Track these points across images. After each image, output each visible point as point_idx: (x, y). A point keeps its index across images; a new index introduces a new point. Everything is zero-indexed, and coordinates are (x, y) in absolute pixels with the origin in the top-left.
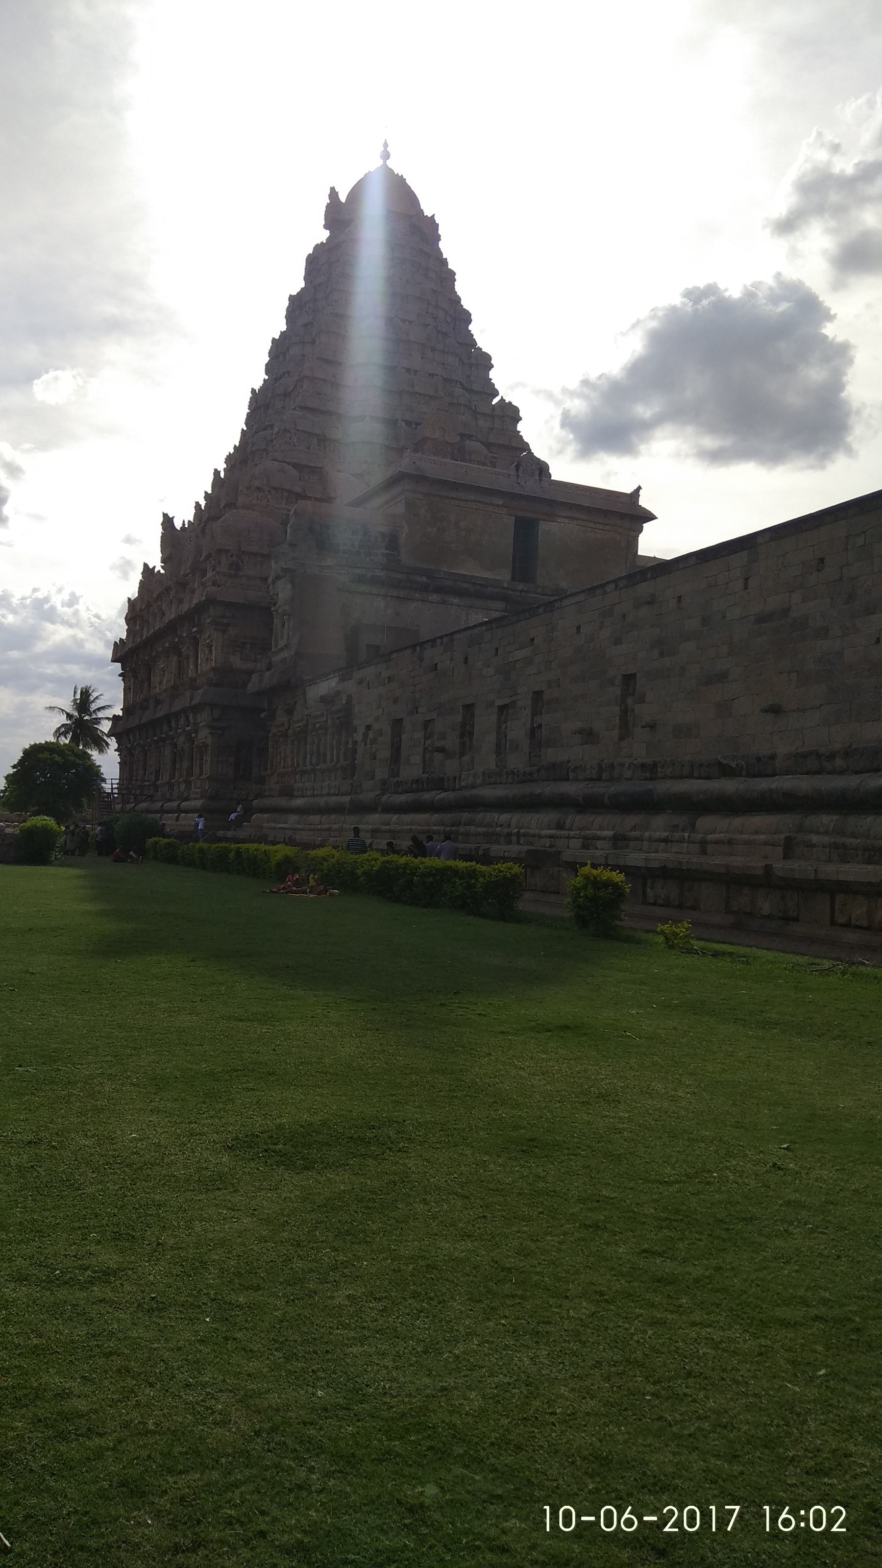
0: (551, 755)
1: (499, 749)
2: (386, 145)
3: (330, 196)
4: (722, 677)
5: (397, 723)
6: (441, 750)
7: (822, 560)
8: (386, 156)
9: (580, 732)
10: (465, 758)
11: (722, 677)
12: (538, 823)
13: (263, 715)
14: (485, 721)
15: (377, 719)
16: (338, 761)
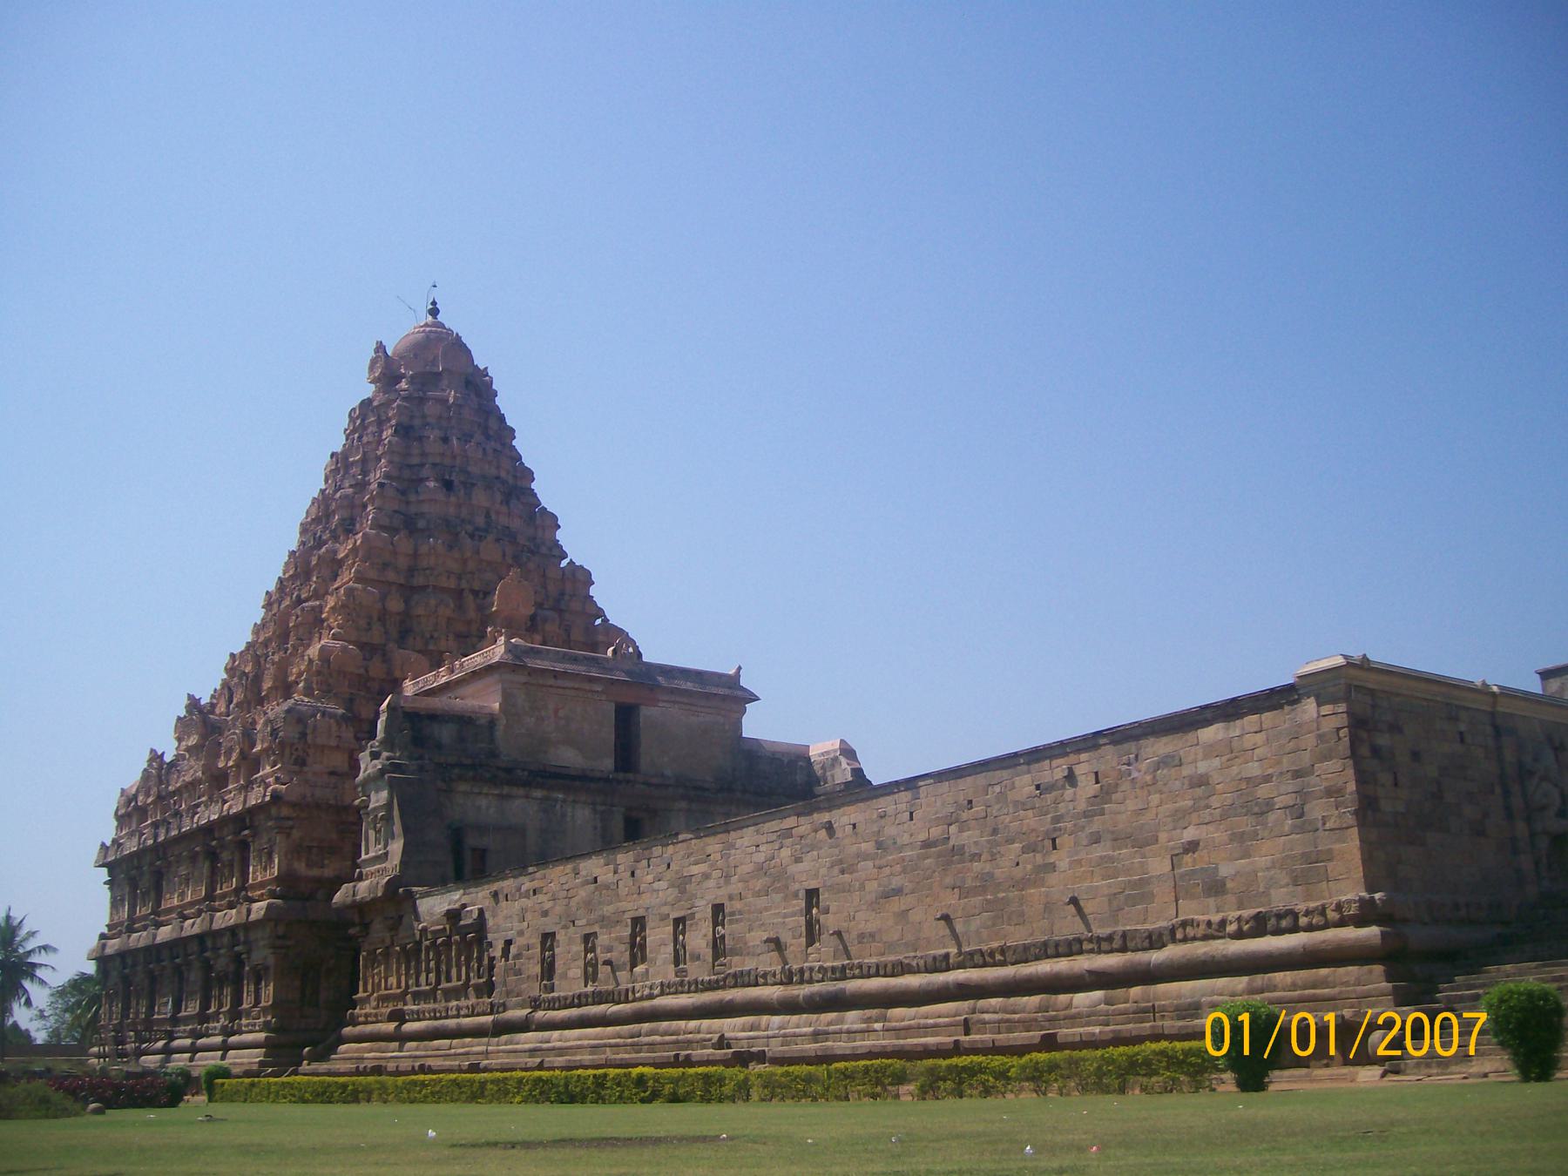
0: (738, 964)
1: (677, 962)
2: (434, 303)
3: (376, 351)
4: (898, 892)
5: (548, 938)
6: (608, 963)
7: (970, 802)
8: (434, 312)
9: (768, 940)
10: (639, 969)
11: (898, 892)
12: (730, 1026)
13: (352, 931)
14: (658, 935)
15: (521, 933)
16: (468, 978)
